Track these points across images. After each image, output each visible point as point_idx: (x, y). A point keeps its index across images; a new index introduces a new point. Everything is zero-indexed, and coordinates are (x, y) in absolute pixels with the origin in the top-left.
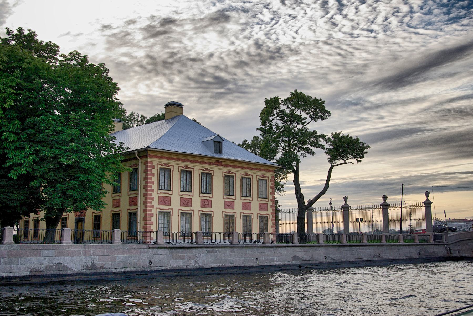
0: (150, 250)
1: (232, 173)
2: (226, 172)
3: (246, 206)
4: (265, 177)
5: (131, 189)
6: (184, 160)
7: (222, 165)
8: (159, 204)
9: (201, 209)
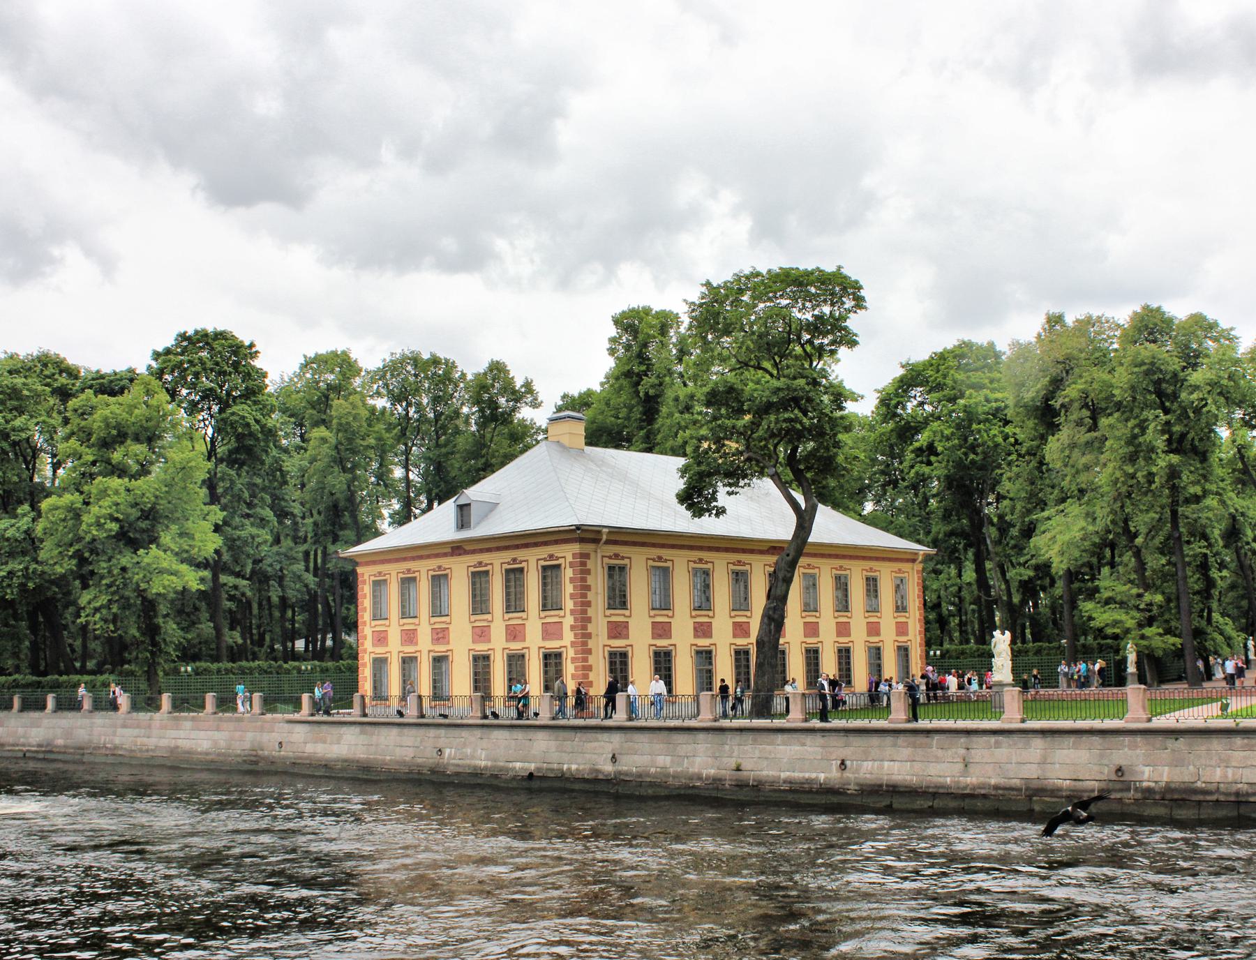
0: (286, 725)
1: (486, 565)
2: (475, 566)
3: (514, 633)
4: (558, 558)
5: (404, 615)
6: (405, 559)
7: (467, 552)
8: (374, 645)
9: (432, 648)
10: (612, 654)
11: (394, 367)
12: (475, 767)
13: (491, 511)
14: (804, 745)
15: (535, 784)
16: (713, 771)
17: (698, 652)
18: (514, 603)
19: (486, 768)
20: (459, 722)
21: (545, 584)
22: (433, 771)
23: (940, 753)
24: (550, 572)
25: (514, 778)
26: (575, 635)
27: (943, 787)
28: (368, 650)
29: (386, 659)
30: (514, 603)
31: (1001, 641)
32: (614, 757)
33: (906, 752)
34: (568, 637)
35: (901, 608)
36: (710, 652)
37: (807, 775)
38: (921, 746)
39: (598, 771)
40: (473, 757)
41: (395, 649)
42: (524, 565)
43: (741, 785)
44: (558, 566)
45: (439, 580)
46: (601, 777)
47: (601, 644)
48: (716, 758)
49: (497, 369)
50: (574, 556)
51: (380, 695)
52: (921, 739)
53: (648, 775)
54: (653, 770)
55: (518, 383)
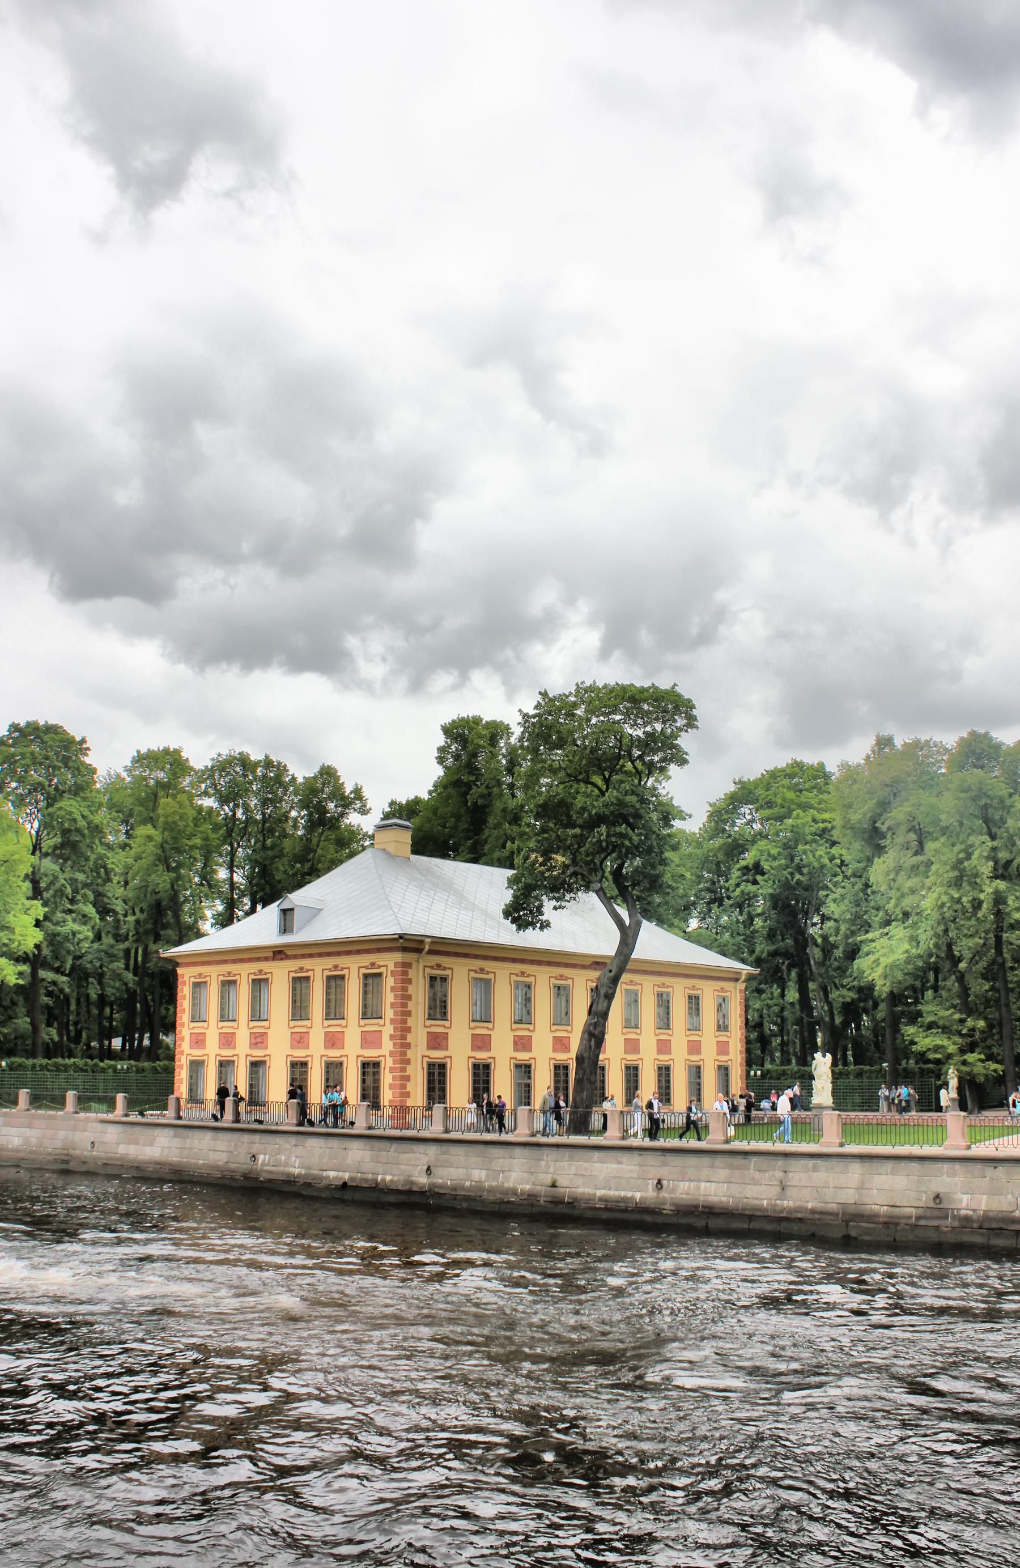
0: (99, 1125)
2: (296, 972)
3: (333, 1040)
5: (223, 1017)
6: (225, 962)
7: (288, 957)
9: (249, 1052)
10: (430, 1065)
11: (223, 766)
12: (289, 1174)
13: (315, 916)
14: (620, 1163)
15: (348, 1196)
16: (528, 1187)
17: (517, 1066)
18: (334, 1010)
19: (299, 1176)
20: (274, 1128)
21: (365, 993)
22: (246, 1177)
23: (757, 1175)
24: (371, 980)
25: (328, 1187)
26: (395, 1044)
27: (760, 1210)
28: (185, 1052)
29: (203, 1062)
30: (334, 1010)
31: (822, 1064)
32: (429, 1169)
33: (723, 1173)
34: (387, 1046)
35: (722, 1027)
36: (529, 1066)
37: (623, 1194)
38: (738, 1168)
39: (413, 1183)
40: (286, 1164)
41: (212, 1052)
42: (345, 972)
43: (557, 1201)
44: (380, 975)
45: (259, 984)
46: (415, 1189)
47: (420, 1054)
48: (532, 1173)
49: (328, 773)
50: (396, 964)
51: (194, 1098)
52: (738, 1161)
53: (463, 1188)
54: (468, 1184)
55: (348, 789)
